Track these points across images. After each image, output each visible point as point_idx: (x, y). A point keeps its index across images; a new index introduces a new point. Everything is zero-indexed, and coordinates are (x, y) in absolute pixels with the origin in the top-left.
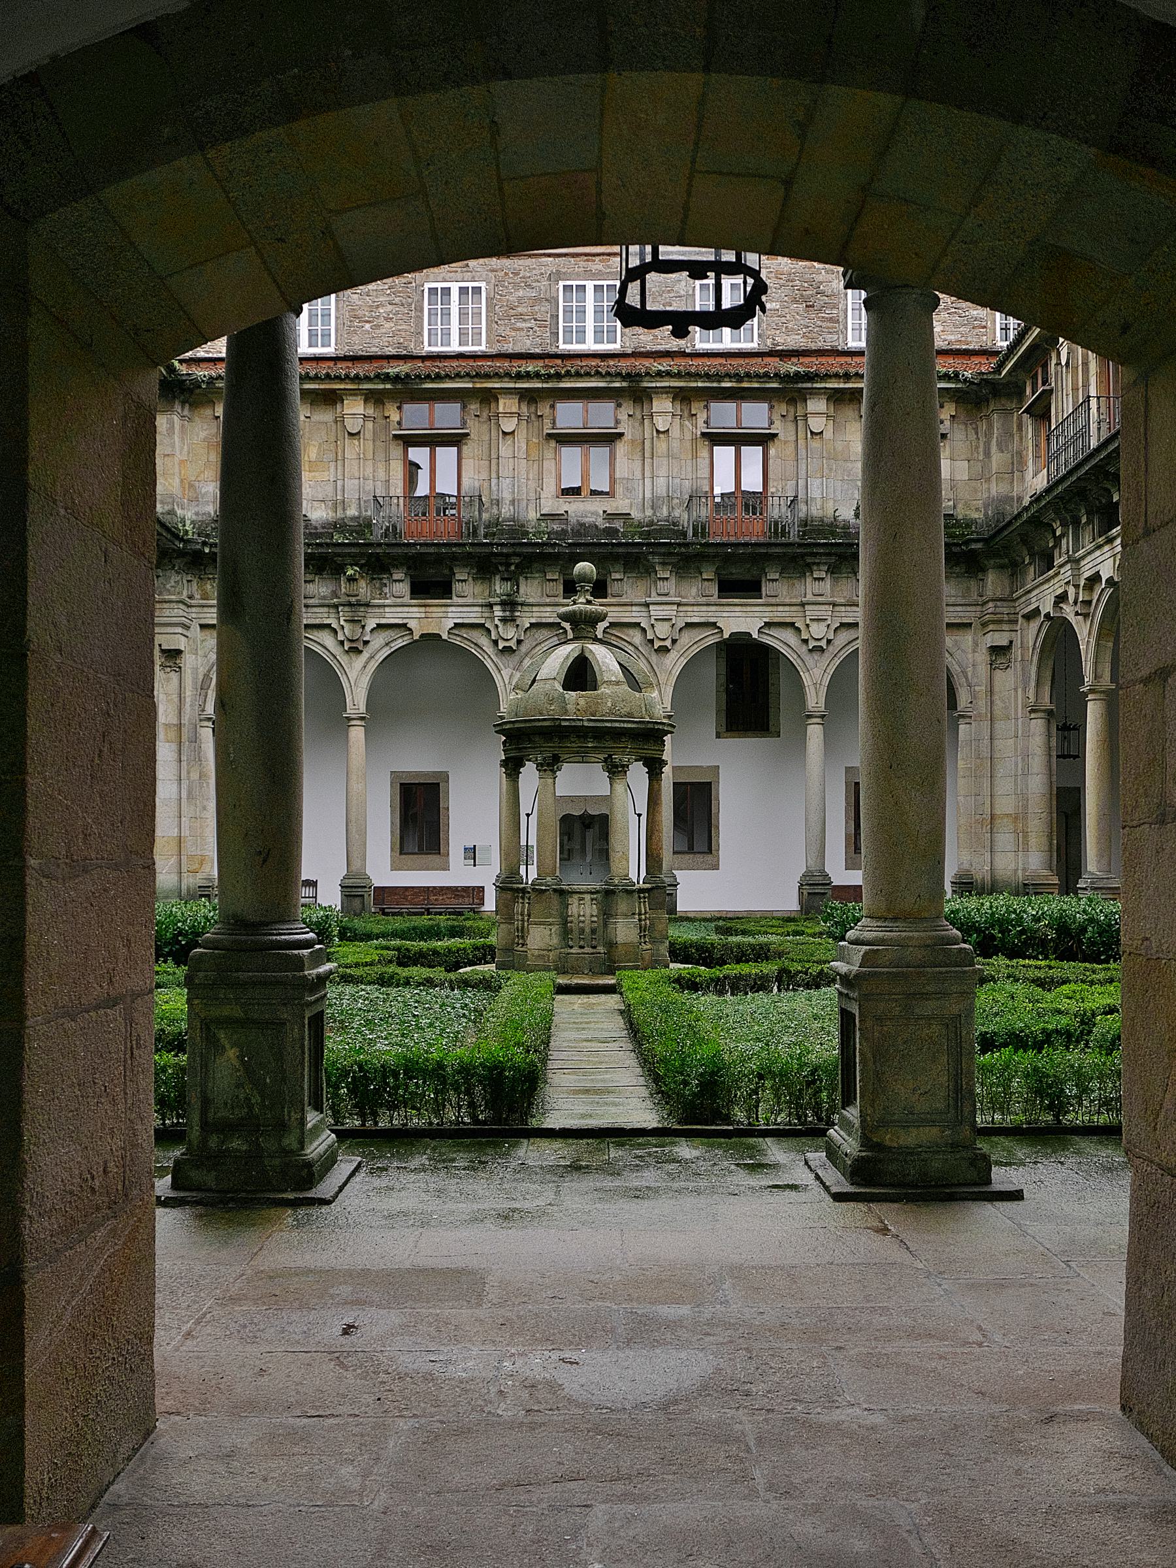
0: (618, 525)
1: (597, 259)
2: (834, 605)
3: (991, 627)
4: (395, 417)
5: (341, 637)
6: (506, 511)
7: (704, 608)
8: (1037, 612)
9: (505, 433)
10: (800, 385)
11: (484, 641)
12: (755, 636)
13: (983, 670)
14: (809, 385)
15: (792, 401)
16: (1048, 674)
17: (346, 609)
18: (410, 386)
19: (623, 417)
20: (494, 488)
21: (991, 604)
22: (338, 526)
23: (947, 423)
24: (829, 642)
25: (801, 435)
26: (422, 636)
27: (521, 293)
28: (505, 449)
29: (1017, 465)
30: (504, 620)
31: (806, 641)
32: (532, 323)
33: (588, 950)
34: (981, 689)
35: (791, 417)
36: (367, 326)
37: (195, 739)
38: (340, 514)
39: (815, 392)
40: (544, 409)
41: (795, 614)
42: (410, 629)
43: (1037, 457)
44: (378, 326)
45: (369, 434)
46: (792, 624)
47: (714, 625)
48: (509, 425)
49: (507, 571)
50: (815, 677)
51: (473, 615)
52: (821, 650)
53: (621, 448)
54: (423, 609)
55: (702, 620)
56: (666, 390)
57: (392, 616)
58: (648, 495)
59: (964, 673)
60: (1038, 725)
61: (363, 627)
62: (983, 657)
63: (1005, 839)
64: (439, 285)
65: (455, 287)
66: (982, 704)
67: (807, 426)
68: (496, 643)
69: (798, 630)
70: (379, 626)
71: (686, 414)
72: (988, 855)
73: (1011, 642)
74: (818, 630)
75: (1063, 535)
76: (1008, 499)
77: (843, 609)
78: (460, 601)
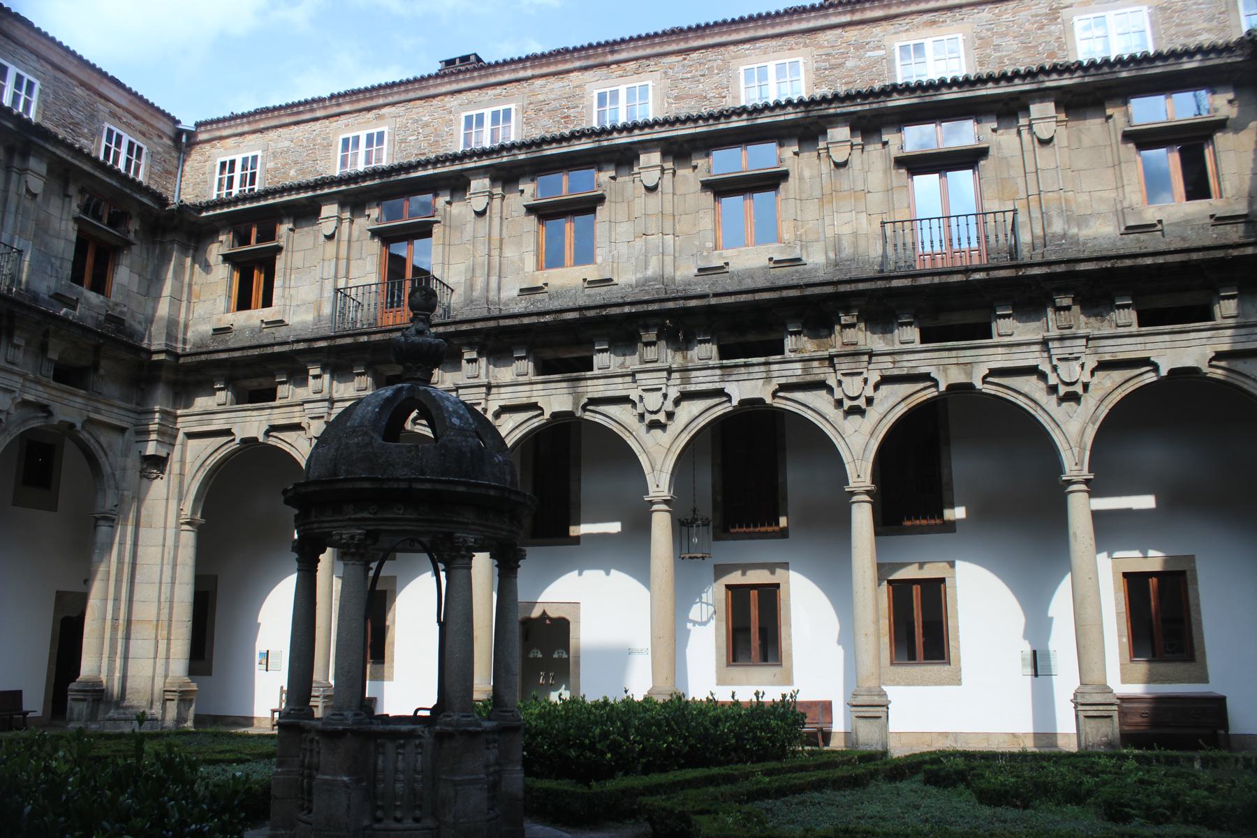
10: (34, 139)
14: (42, 143)
59: (113, 475)
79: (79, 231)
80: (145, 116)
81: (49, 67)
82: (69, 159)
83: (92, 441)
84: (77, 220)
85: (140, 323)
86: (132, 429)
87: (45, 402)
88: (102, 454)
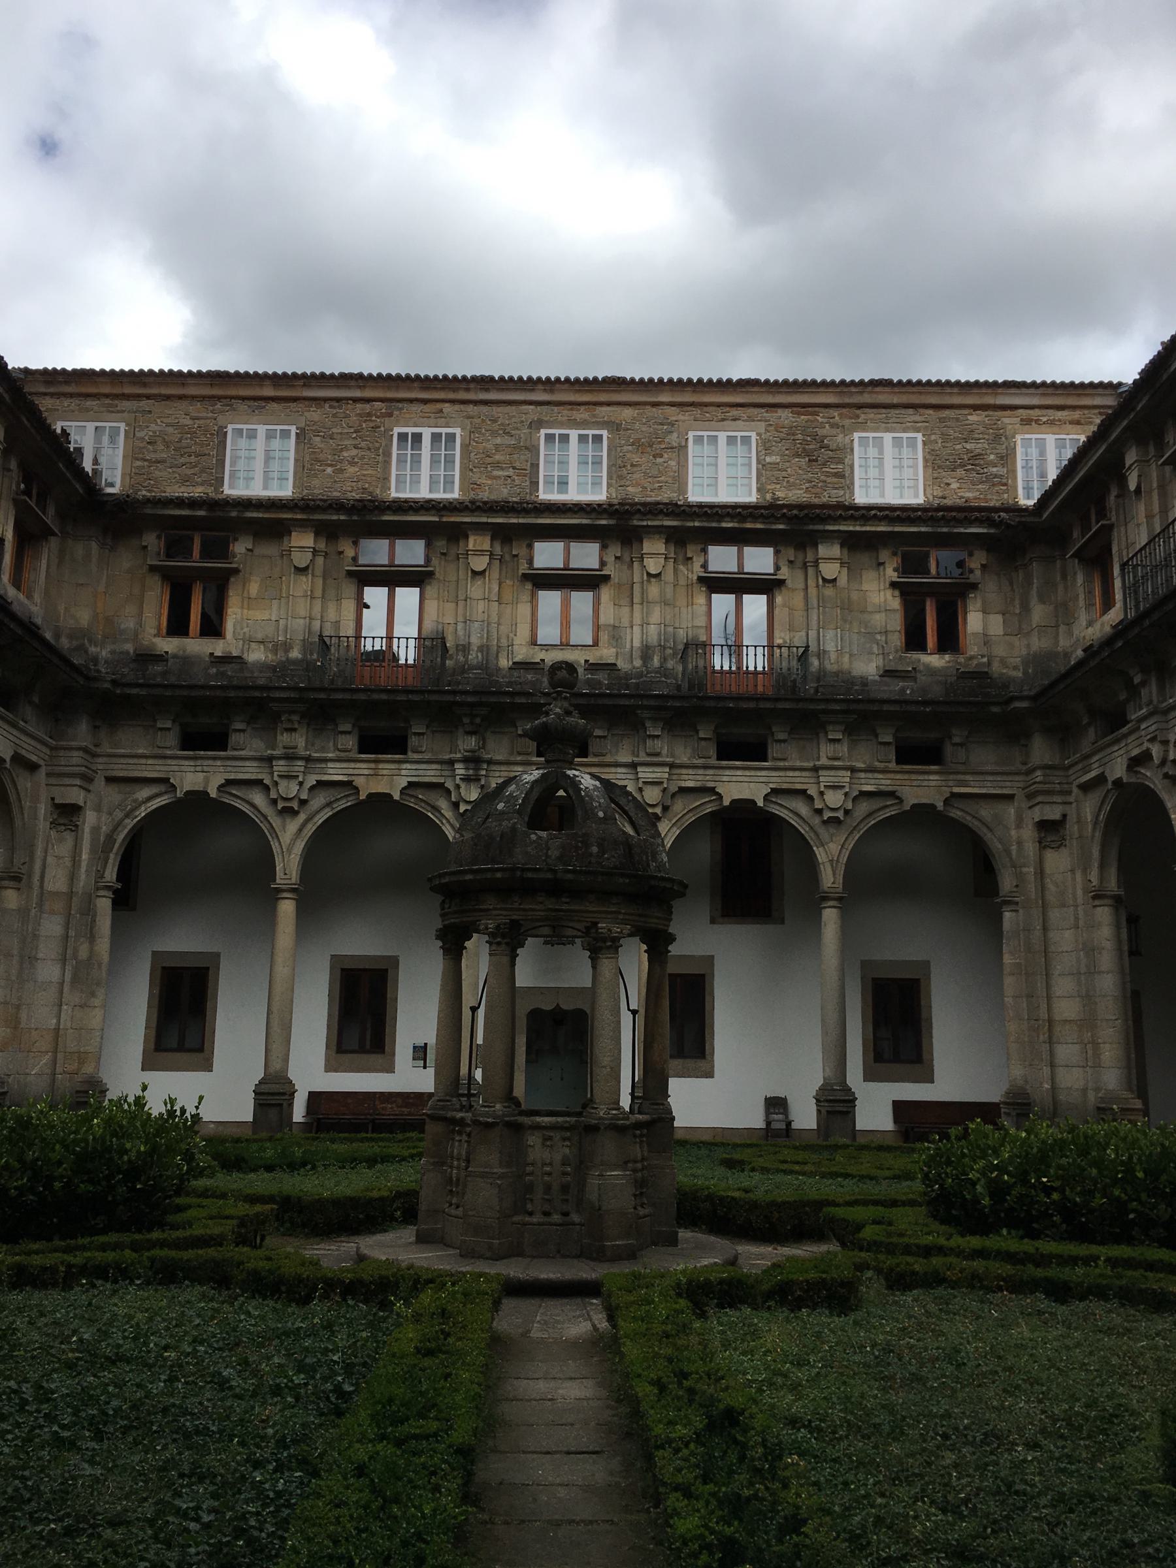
0: (603, 677)
1: (582, 408)
2: (853, 770)
3: (1039, 799)
4: (350, 553)
5: (273, 795)
6: (474, 657)
7: (701, 772)
8: (1101, 779)
9: (475, 573)
10: (811, 527)
11: (443, 804)
12: (760, 803)
13: (1031, 848)
14: (820, 527)
15: (801, 546)
16: (1114, 854)
17: (282, 762)
18: (368, 518)
19: (610, 559)
20: (461, 633)
21: (1038, 773)
22: (280, 669)
23: (978, 573)
24: (847, 812)
25: (811, 583)
26: (370, 795)
27: (499, 441)
28: (476, 589)
29: (1064, 614)
30: (467, 779)
31: (819, 812)
32: (511, 472)
33: (556, 1218)
34: (1030, 870)
35: (799, 563)
36: (329, 470)
37: (89, 911)
38: (281, 656)
39: (828, 536)
40: (519, 549)
41: (806, 780)
42: (356, 788)
43: (1090, 605)
44: (341, 471)
45: (319, 570)
46: (804, 792)
47: (712, 790)
48: (479, 563)
49: (472, 723)
50: (831, 855)
51: (430, 774)
52: (835, 821)
53: (606, 593)
54: (372, 765)
55: (699, 784)
56: (659, 530)
57: (336, 772)
58: (637, 643)
59: (1008, 852)
60: (1104, 914)
61: (301, 784)
62: (1028, 833)
63: (1067, 1052)
64: (410, 430)
65: (427, 433)
66: (1032, 888)
67: (818, 572)
68: (456, 805)
69: (811, 798)
70: (320, 784)
71: (681, 557)
72: (1046, 1070)
73: (1064, 816)
74: (834, 799)
75: (1144, 683)
76: (1052, 655)
77: (862, 775)
78: (416, 756)
79: (902, 594)
80: (1071, 401)
81: (931, 412)
82: (858, 528)
83: (969, 818)
84: (894, 585)
85: (1015, 668)
86: (1020, 795)
87: (890, 788)
88: (985, 830)
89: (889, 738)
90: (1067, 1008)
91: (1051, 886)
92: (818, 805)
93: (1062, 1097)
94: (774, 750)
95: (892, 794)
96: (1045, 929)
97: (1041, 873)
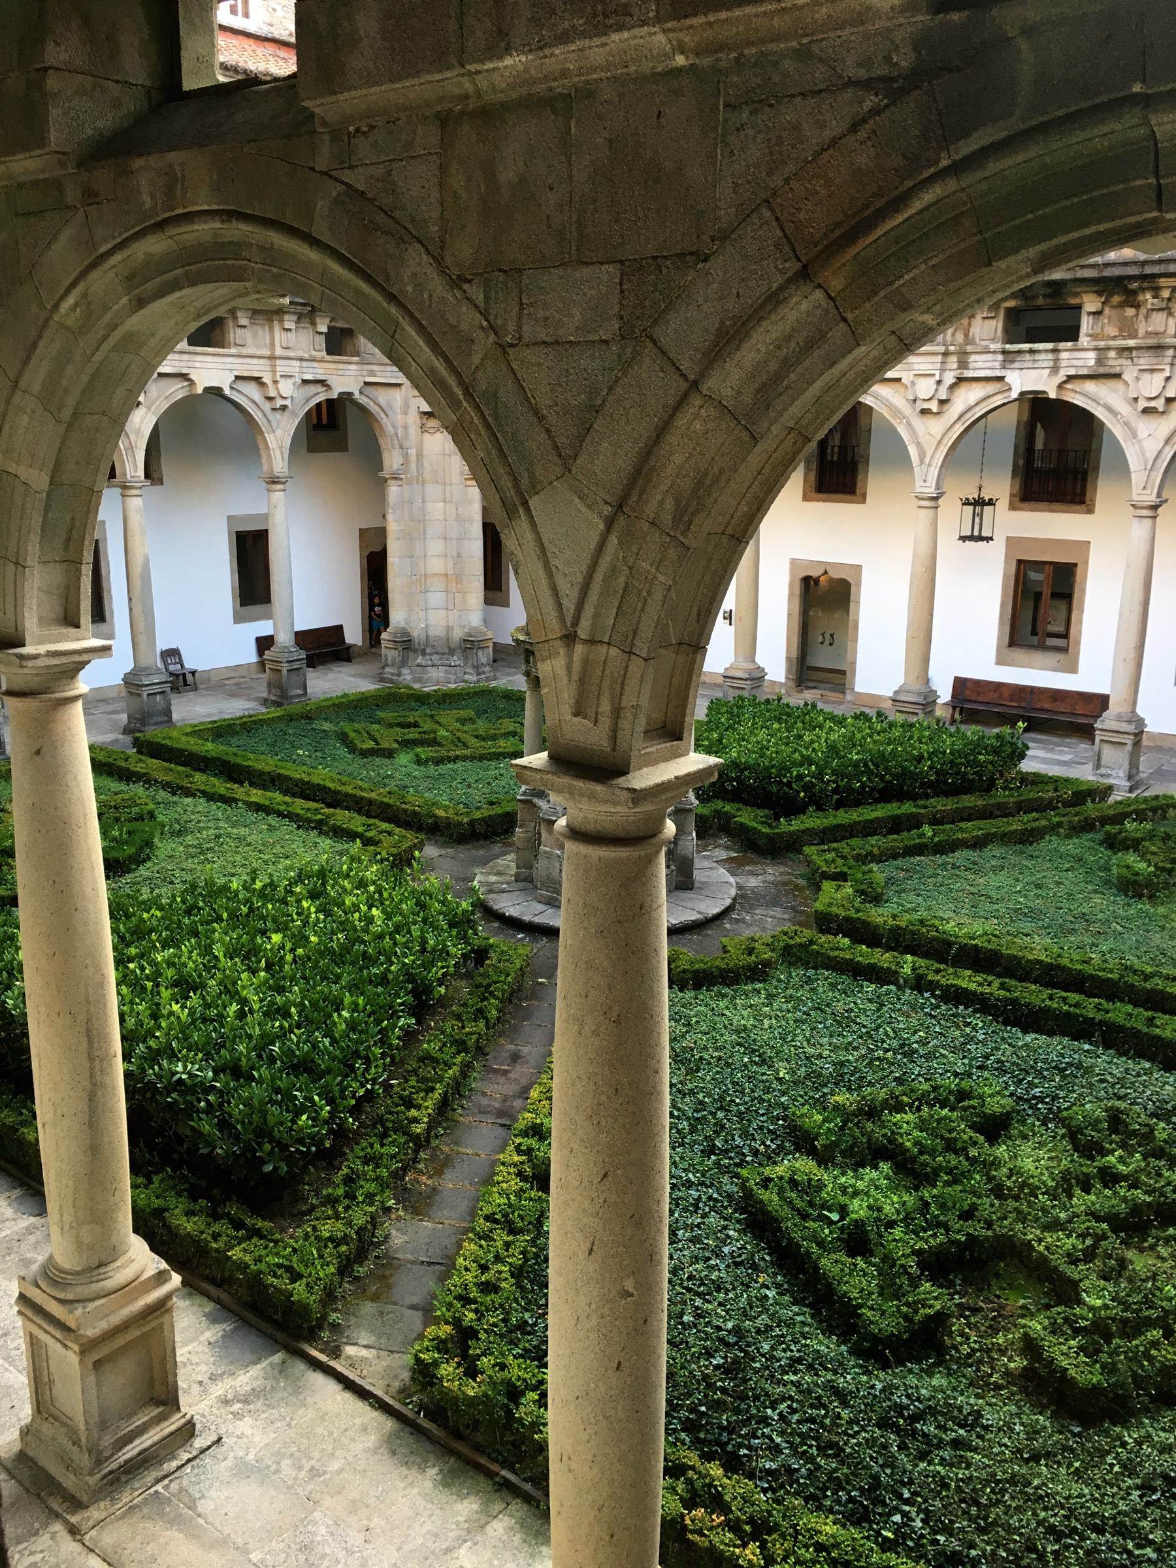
13: (414, 431)
31: (270, 399)
47: (184, 376)
63: (436, 598)
89: (324, 329)
90: (436, 565)
91: (426, 465)
92: (272, 393)
93: (431, 633)
94: (234, 334)
95: (322, 382)
96: (424, 501)
97: (420, 456)
